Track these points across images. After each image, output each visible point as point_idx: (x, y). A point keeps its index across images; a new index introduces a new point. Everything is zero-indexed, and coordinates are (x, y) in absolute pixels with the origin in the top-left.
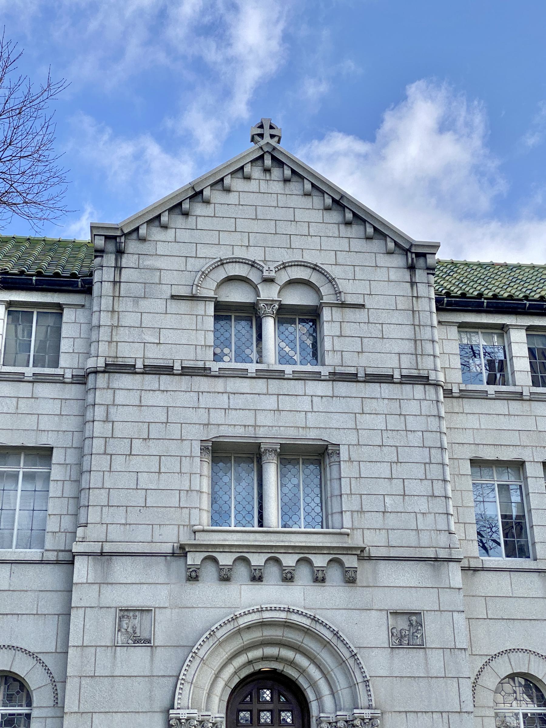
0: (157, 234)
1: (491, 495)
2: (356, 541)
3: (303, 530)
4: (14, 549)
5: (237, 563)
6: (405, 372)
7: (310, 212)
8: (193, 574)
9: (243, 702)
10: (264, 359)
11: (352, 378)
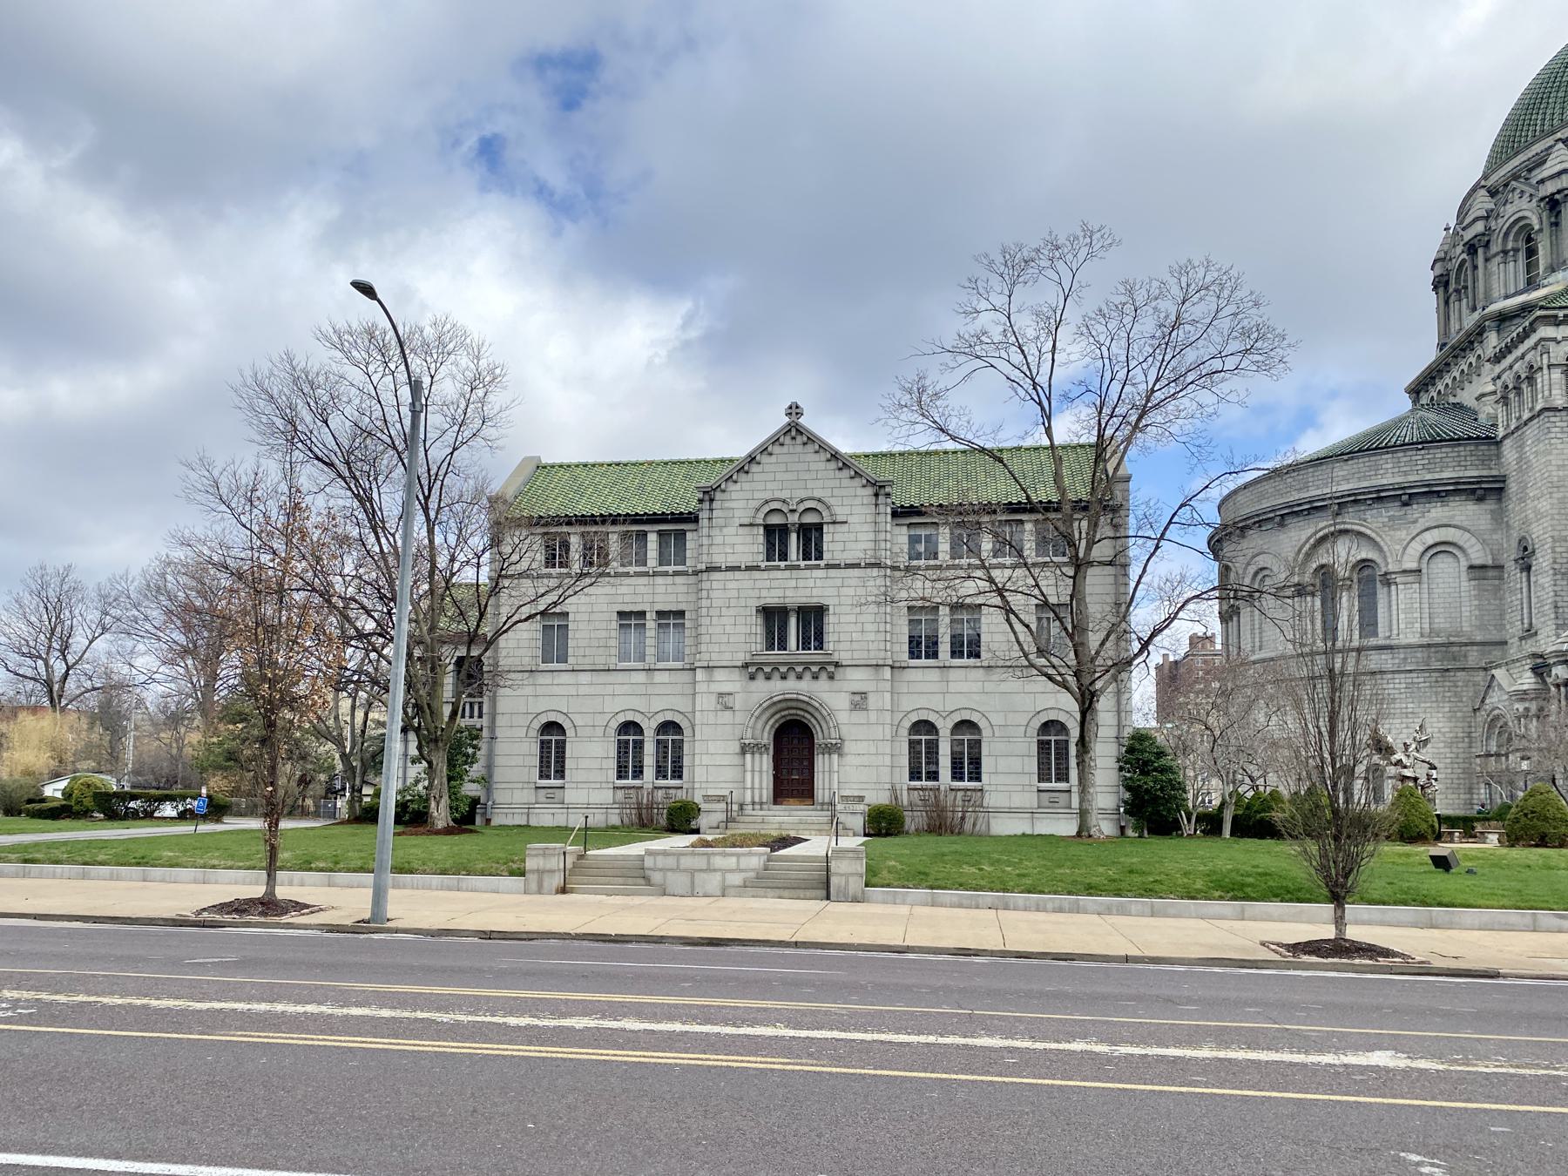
0: (731, 487)
2: (835, 658)
7: (819, 463)
11: (837, 566)
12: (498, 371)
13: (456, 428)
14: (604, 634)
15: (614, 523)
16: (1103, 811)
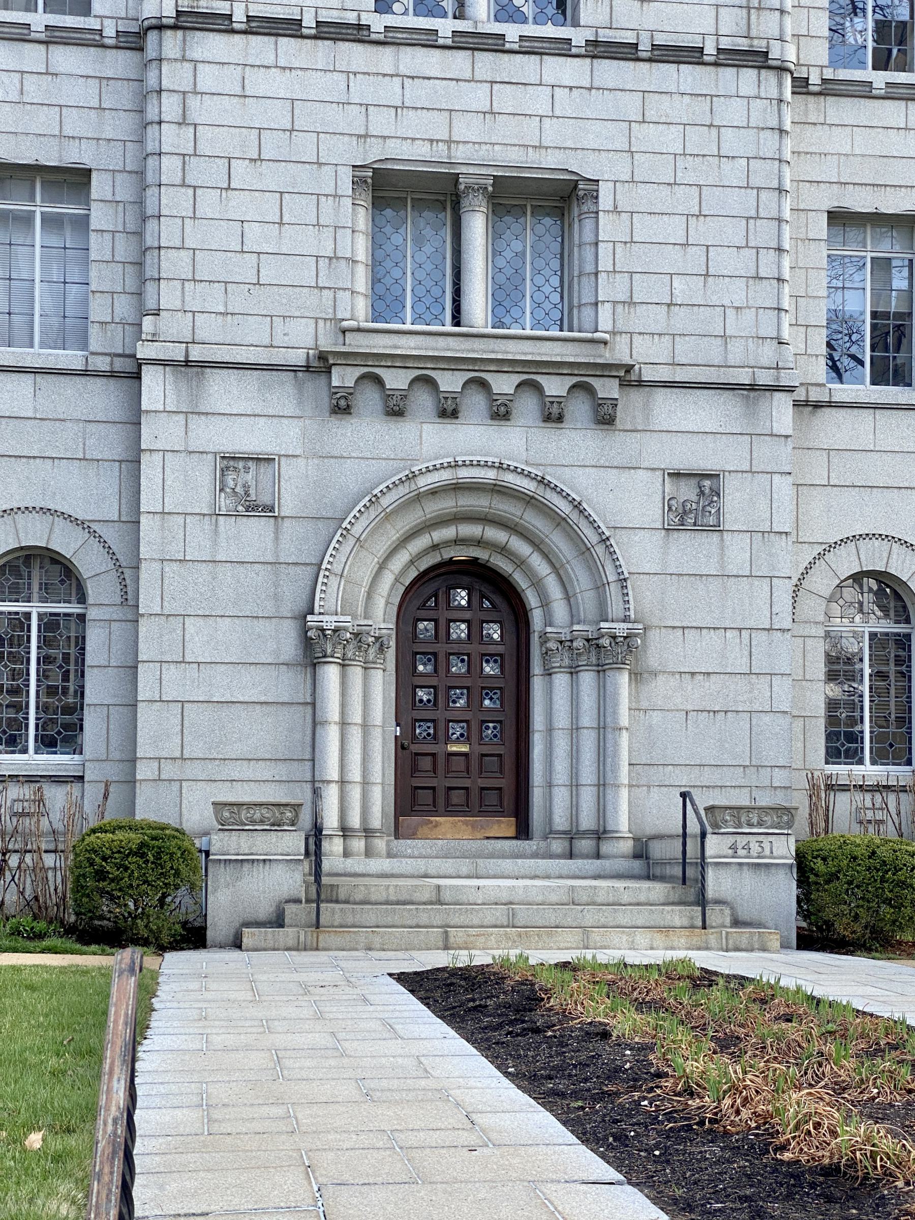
1: (857, 277)
2: (620, 353)
3: (528, 332)
4: (36, 349)
5: (415, 387)
6: (725, 43)
8: (343, 403)
9: (423, 606)
10: (469, 11)
11: (626, 52)
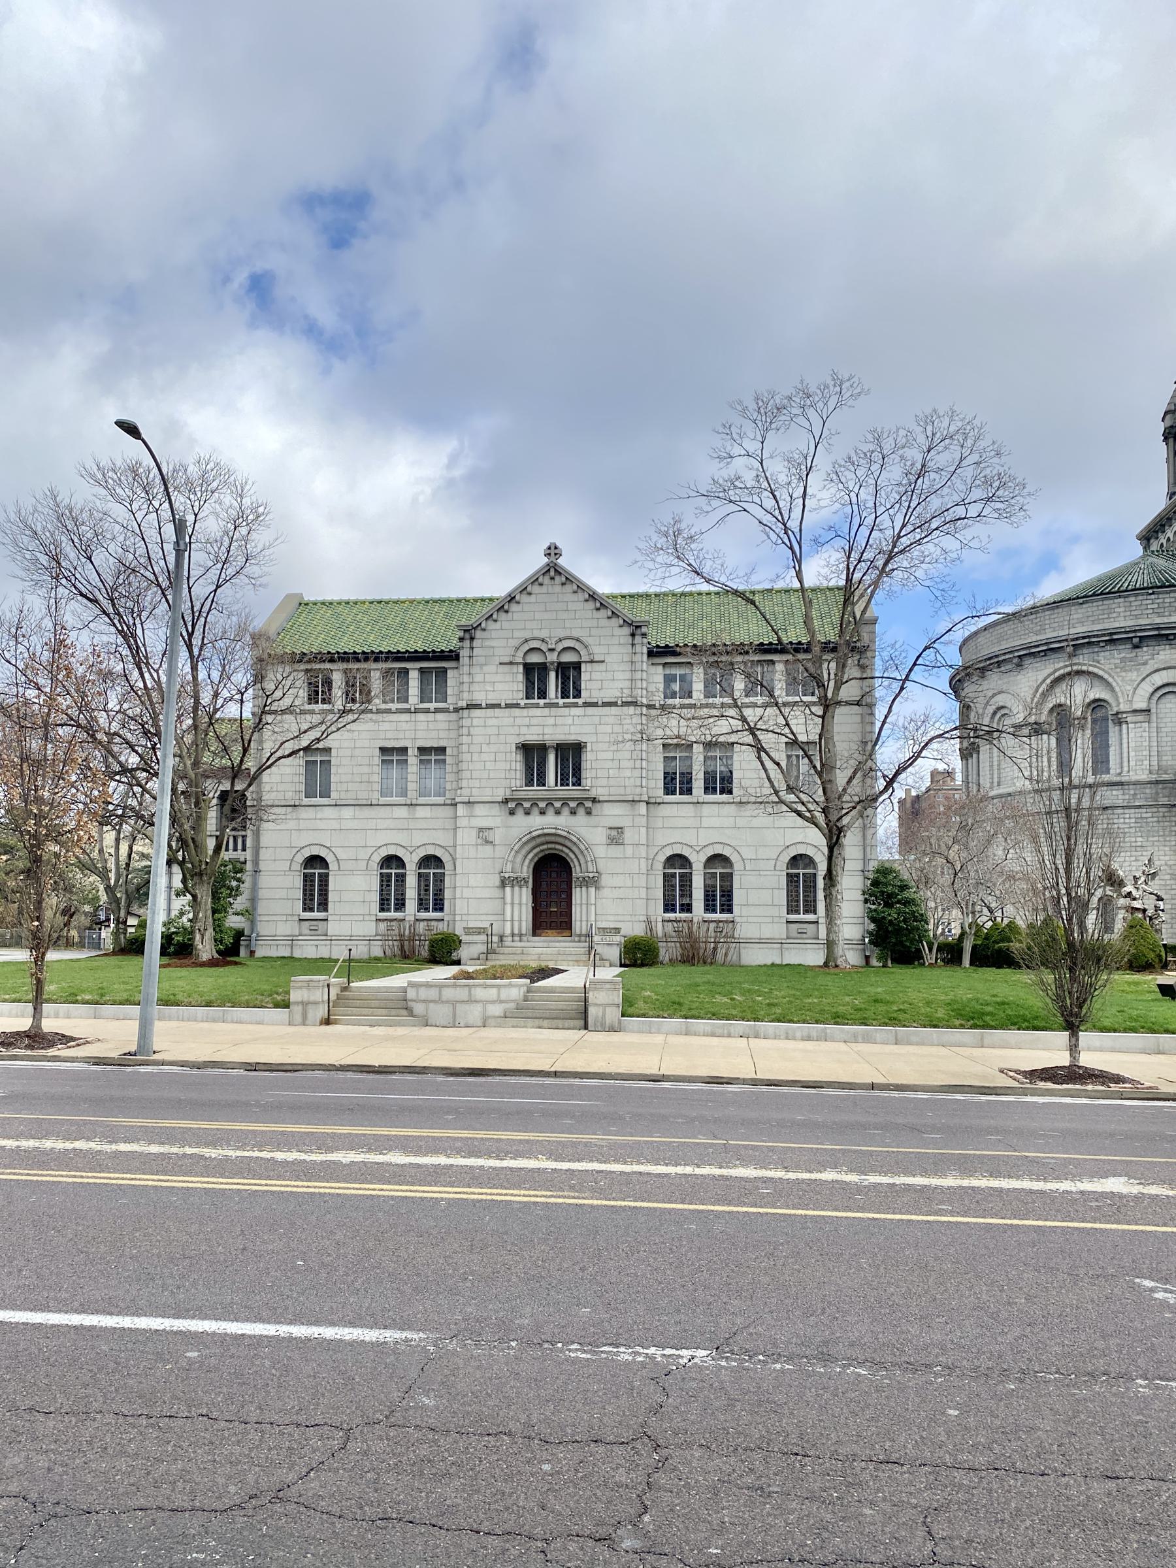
0: (491, 625)
2: (593, 794)
7: (576, 601)
11: (595, 705)
12: (261, 510)
13: (219, 566)
14: (366, 770)
15: (376, 660)
16: (849, 942)
